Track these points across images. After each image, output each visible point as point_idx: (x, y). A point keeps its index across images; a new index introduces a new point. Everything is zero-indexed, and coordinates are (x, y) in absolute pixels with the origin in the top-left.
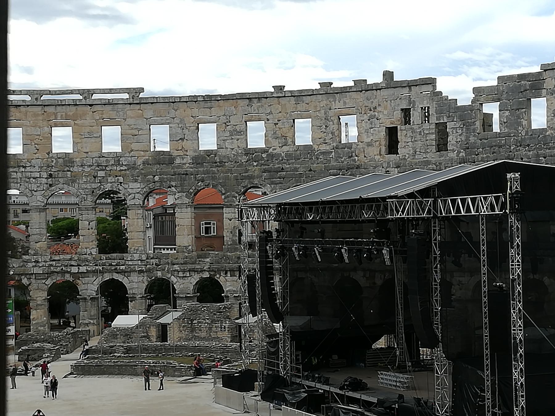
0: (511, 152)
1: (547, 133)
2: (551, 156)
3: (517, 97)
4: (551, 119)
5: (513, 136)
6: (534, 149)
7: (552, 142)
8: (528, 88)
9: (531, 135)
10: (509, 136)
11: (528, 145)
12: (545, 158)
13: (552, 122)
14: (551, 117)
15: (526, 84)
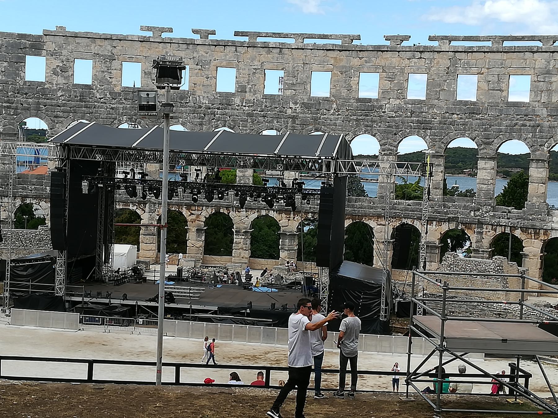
0: (8, 97)
1: (46, 87)
2: (52, 106)
3: (16, 52)
4: (50, 75)
5: (11, 84)
6: (32, 97)
7: (50, 94)
8: (28, 46)
9: (29, 86)
10: (7, 84)
11: (26, 94)
12: (45, 106)
13: (50, 78)
14: (50, 74)
15: (25, 43)
